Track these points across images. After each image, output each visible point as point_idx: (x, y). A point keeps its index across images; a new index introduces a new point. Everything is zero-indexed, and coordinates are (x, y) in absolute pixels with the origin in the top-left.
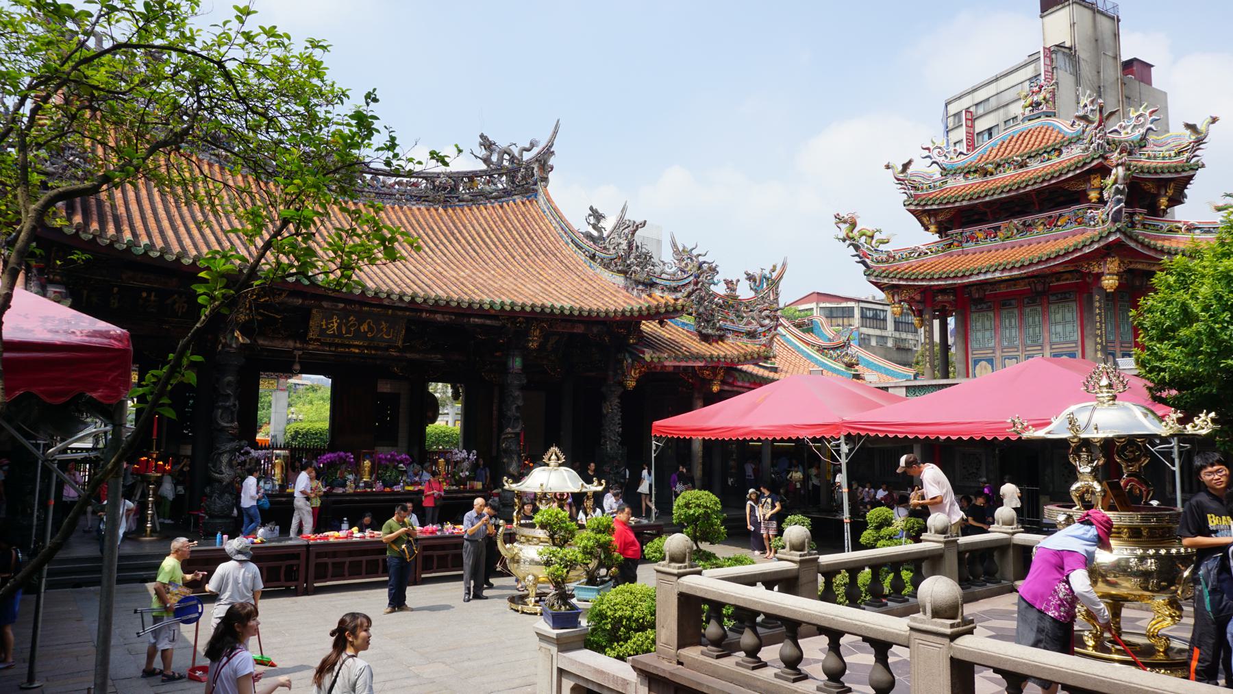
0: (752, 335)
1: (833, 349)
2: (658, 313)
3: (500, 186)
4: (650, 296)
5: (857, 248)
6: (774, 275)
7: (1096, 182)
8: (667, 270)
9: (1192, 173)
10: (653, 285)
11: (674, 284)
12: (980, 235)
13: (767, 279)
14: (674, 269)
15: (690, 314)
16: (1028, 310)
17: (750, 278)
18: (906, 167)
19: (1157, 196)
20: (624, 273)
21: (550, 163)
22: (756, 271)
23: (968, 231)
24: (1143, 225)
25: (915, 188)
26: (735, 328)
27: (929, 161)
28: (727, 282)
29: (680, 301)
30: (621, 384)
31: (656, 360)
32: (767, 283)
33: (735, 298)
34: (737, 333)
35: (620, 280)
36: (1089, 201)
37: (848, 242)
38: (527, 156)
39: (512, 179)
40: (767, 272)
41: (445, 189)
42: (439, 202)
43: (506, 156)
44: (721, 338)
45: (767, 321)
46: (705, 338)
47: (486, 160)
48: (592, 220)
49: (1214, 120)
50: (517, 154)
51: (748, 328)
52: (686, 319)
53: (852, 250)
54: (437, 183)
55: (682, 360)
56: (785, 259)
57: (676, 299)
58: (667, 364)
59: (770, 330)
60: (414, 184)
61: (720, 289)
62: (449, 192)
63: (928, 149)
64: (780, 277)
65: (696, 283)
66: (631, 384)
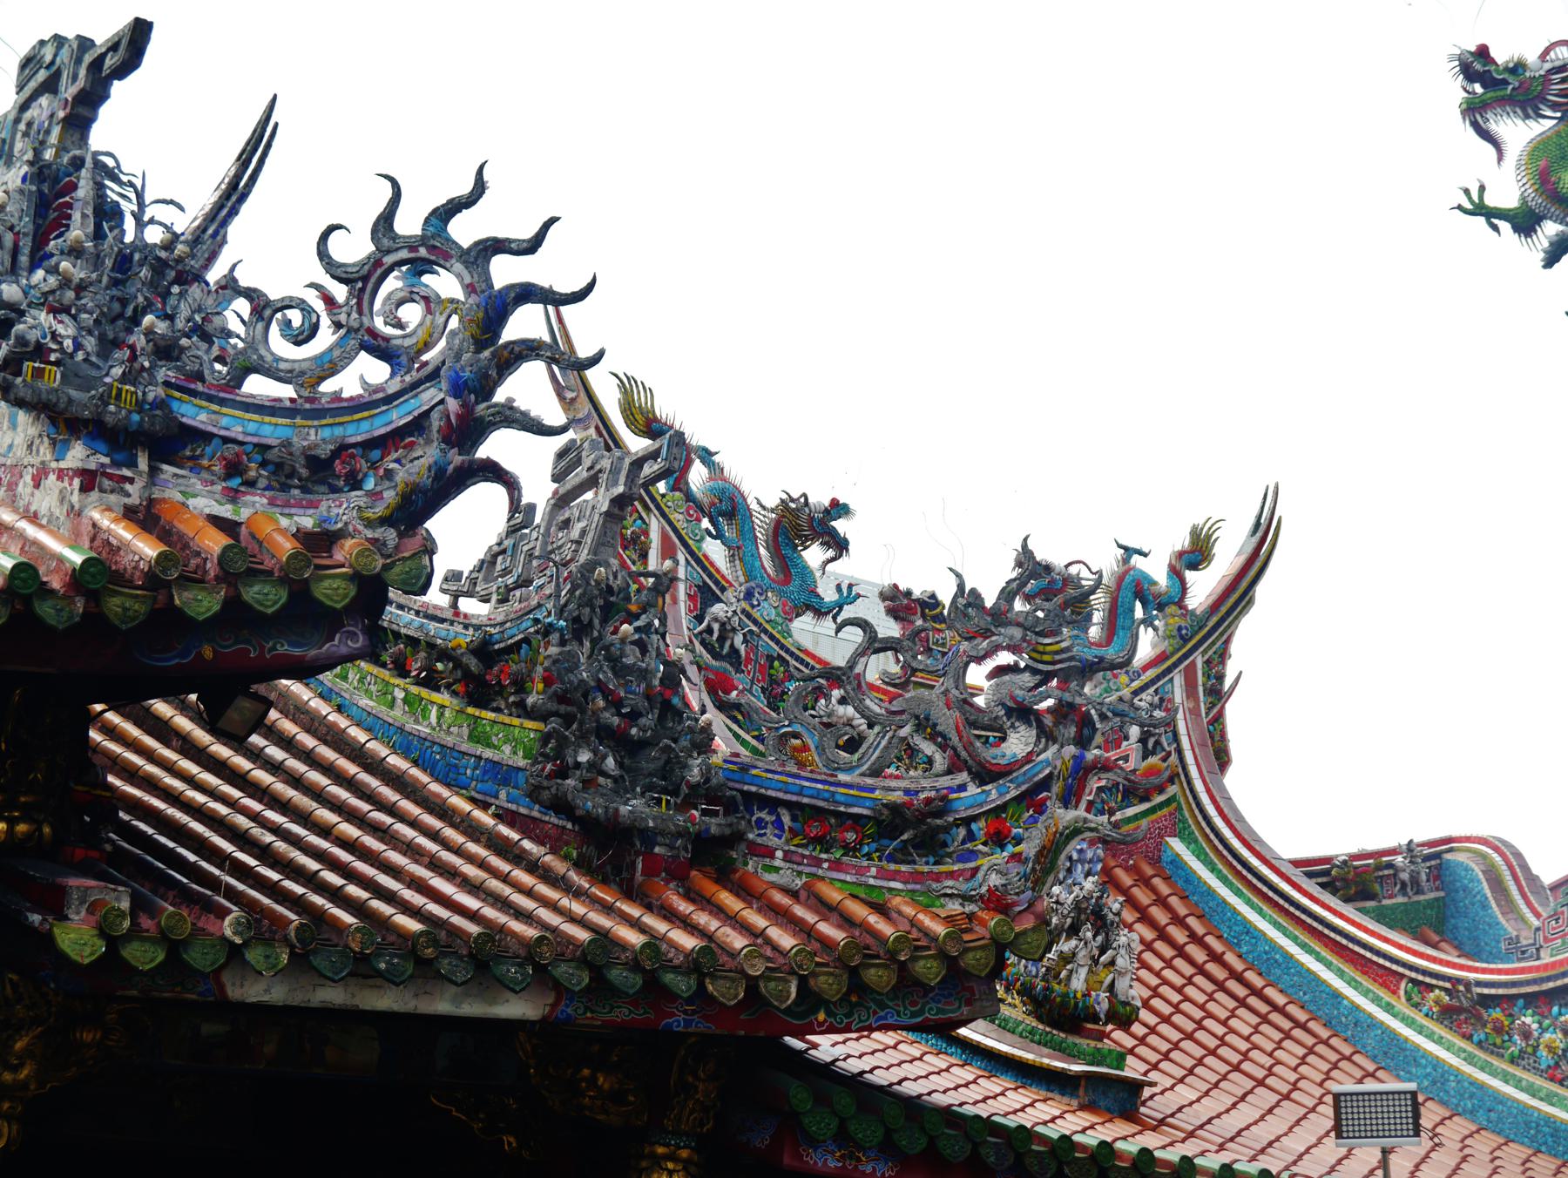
1: (1539, 1001)
2: (167, 622)
4: (146, 517)
6: (1202, 587)
8: (279, 346)
10: (172, 443)
11: (319, 437)
13: (1157, 602)
14: (326, 338)
26: (811, 790)
29: (345, 551)
31: (144, 956)
40: (1156, 570)
44: (714, 860)
46: (609, 853)
51: (895, 788)
55: (362, 969)
56: (1271, 497)
57: (320, 541)
59: (1032, 799)
64: (1238, 594)
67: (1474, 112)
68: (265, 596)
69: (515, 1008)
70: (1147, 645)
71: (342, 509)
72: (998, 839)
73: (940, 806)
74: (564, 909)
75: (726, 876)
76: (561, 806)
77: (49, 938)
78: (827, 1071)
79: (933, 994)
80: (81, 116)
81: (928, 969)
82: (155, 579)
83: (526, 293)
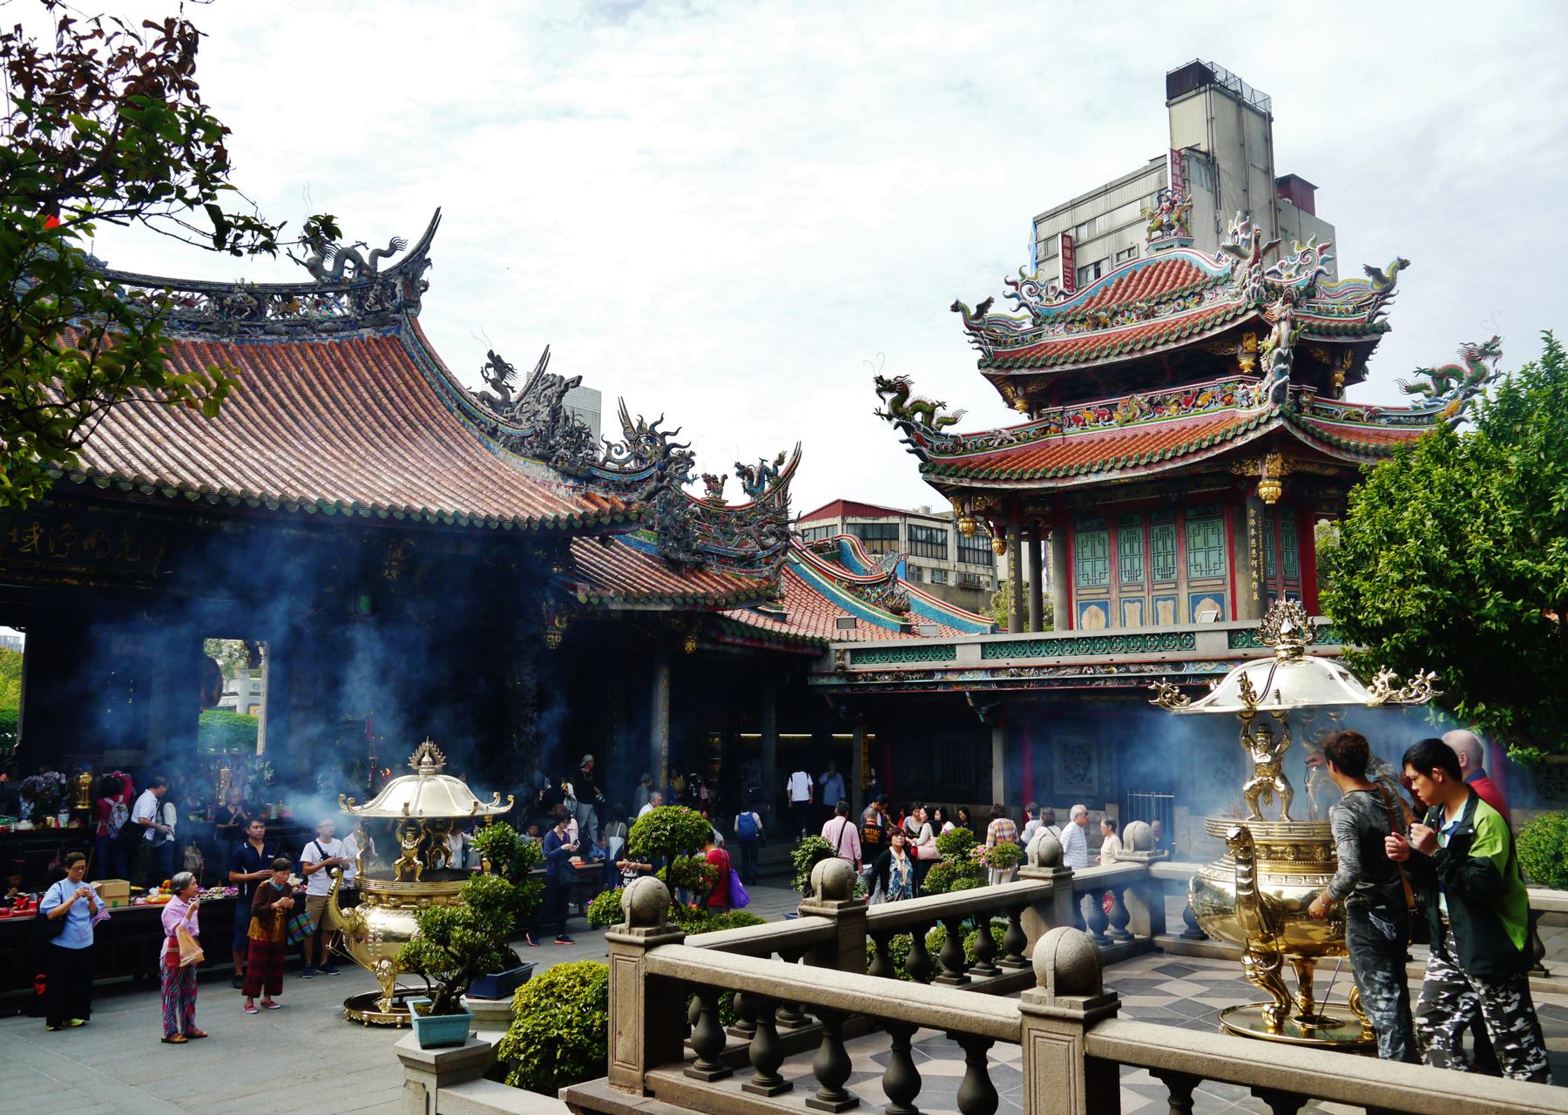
0: (748, 561)
1: (872, 586)
2: (599, 525)
3: (338, 312)
4: (587, 497)
5: (908, 429)
6: (782, 469)
7: (1250, 344)
9: (1375, 337)
10: (592, 479)
11: (627, 479)
12: (1089, 417)
14: (625, 455)
15: (651, 528)
16: (1157, 530)
17: (743, 472)
18: (982, 308)
19: (1331, 369)
20: (545, 458)
21: (424, 278)
22: (752, 462)
23: (1071, 410)
24: (1313, 409)
25: (995, 342)
26: (722, 551)
27: (1015, 302)
28: (710, 480)
29: (635, 506)
30: (538, 639)
31: (595, 601)
32: (769, 482)
33: (720, 504)
34: (724, 559)
35: (540, 471)
36: (1240, 371)
37: (895, 420)
38: (384, 264)
39: (358, 303)
40: (770, 465)
41: (241, 311)
42: (231, 333)
43: (349, 263)
44: (699, 568)
45: (772, 541)
46: (675, 566)
47: (314, 268)
48: (492, 374)
49: (1403, 264)
50: (367, 261)
51: (741, 551)
52: (643, 536)
53: (901, 434)
54: (228, 301)
55: (637, 601)
56: (799, 444)
57: (628, 504)
58: (613, 607)
59: (775, 554)
60: (186, 302)
61: (697, 490)
62: (248, 318)
63: (1014, 284)
65: (661, 479)
66: (554, 639)
67: (879, 391)
68: (619, 519)
69: (666, 608)
70: (767, 486)
71: (634, 496)
72: (767, 564)
73: (754, 555)
74: (674, 585)
75: (701, 571)
76: (666, 556)
77: (575, 598)
78: (729, 619)
79: (753, 600)
80: (561, 395)
81: (753, 595)
82: (596, 516)
83: (675, 445)
